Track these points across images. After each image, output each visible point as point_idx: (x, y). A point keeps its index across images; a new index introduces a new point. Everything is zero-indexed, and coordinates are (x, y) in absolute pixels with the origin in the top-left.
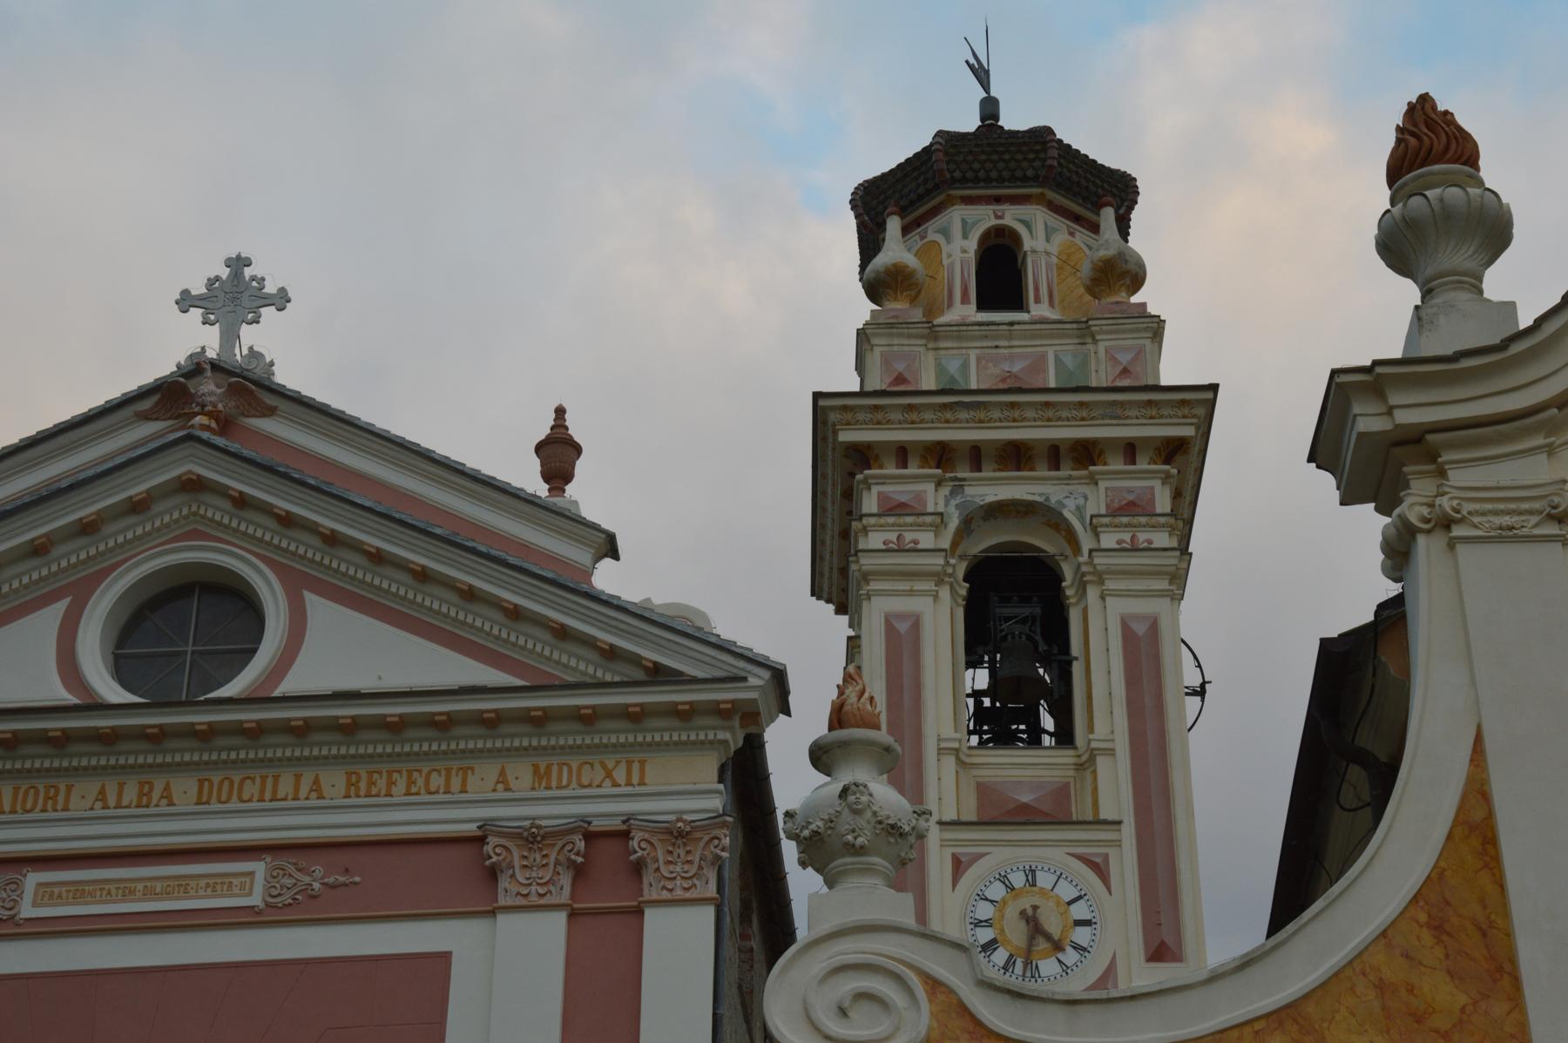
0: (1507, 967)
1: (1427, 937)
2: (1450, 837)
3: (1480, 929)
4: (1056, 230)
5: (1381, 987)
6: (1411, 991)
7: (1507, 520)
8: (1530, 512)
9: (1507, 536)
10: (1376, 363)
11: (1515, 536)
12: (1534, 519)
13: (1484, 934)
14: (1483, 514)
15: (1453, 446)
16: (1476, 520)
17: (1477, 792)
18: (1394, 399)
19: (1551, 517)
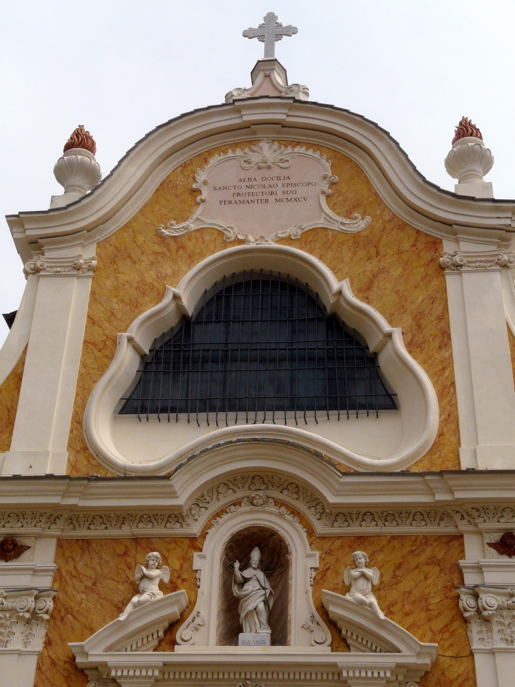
0: (12, 422)
2: (8, 378)
3: (8, 409)
7: (59, 269)
8: (68, 266)
9: (57, 275)
10: (20, 213)
11: (60, 275)
12: (69, 269)
13: (9, 411)
14: (52, 267)
15: (48, 244)
16: (48, 269)
17: (22, 362)
18: (26, 227)
19: (75, 268)
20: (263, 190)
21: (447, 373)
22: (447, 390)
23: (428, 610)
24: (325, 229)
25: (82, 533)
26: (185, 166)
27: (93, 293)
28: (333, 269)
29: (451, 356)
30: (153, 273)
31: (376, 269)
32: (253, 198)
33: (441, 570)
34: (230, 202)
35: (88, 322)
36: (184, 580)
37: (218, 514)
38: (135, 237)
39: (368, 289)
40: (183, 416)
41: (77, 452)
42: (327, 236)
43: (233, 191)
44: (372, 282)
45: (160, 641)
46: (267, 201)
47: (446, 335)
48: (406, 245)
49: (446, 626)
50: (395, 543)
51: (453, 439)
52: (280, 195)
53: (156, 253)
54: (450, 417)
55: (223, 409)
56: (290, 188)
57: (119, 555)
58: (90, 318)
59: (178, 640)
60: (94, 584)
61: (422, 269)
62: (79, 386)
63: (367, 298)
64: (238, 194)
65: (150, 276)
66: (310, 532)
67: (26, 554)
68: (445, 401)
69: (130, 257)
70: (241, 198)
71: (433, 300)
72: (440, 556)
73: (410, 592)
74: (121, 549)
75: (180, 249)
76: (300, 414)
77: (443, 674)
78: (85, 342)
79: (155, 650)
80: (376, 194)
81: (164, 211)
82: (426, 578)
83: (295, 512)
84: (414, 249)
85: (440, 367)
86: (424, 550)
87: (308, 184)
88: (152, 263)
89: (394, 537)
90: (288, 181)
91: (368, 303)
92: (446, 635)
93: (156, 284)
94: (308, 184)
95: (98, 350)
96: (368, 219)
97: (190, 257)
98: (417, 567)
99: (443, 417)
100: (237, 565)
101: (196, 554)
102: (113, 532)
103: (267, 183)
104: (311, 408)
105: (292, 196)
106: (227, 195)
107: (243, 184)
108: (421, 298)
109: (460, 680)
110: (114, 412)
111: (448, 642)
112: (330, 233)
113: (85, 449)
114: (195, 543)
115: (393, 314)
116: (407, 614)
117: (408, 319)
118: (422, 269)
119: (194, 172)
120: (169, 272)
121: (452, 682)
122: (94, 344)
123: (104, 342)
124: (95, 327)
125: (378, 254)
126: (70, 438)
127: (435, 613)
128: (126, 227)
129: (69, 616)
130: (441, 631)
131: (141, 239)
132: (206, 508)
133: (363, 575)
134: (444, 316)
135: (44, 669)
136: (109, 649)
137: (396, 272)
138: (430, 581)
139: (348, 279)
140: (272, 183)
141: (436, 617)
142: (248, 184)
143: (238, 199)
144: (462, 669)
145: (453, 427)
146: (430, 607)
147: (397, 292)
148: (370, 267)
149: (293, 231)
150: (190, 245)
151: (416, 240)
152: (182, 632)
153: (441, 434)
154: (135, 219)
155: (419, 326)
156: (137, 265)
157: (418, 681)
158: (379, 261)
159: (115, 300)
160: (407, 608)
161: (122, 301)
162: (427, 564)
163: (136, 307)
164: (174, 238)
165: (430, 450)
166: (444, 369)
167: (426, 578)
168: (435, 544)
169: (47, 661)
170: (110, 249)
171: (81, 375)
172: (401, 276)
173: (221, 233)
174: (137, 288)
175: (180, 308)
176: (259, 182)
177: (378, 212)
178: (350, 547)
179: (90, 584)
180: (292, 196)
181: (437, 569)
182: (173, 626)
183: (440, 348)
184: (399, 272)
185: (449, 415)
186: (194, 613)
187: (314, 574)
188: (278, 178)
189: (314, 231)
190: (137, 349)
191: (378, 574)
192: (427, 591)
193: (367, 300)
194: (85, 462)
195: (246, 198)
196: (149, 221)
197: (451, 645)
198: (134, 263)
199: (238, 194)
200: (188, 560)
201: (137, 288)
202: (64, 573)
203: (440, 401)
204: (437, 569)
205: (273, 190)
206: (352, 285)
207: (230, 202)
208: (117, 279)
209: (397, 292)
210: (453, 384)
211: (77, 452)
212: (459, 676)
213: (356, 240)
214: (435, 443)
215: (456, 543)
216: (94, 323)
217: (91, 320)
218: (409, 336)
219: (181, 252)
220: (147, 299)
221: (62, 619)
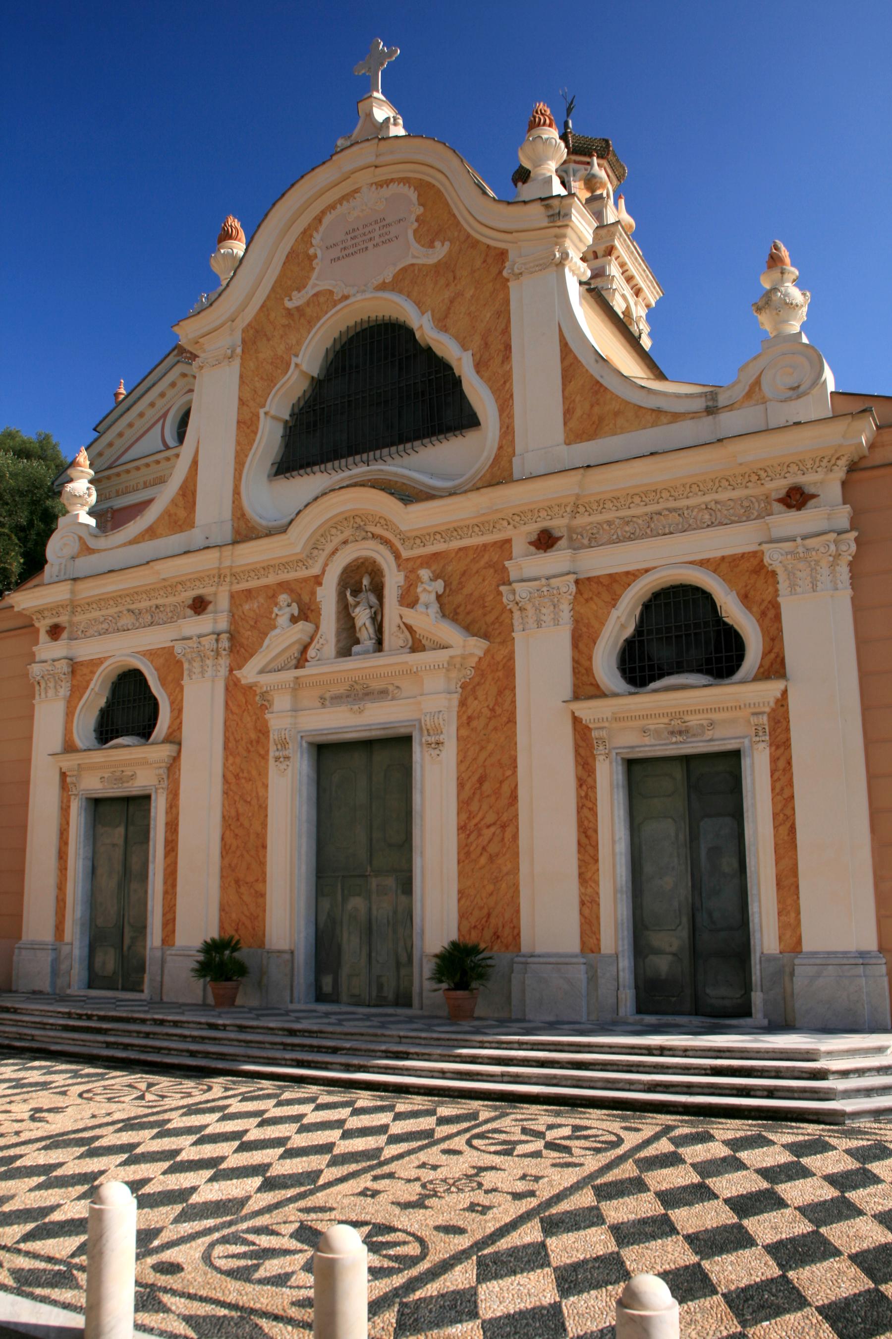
1: (181, 499)
4: (578, 171)
5: (170, 515)
6: (176, 514)
20: (365, 238)
21: (508, 384)
22: (505, 404)
23: (484, 607)
24: (413, 265)
25: (244, 586)
26: (304, 232)
27: (241, 377)
28: (418, 304)
29: (511, 368)
30: (282, 347)
31: (453, 295)
32: (356, 249)
33: (496, 571)
34: (339, 258)
35: (239, 404)
36: (312, 611)
37: (334, 553)
38: (268, 315)
39: (446, 317)
40: (316, 468)
41: (239, 519)
42: (414, 271)
43: (342, 246)
44: (449, 308)
45: (299, 661)
46: (367, 248)
47: (508, 347)
48: (478, 263)
49: (497, 618)
50: (461, 554)
51: (510, 450)
52: (377, 240)
53: (283, 326)
54: (507, 430)
55: (350, 454)
56: (385, 230)
57: (270, 598)
58: (240, 399)
59: (309, 659)
60: (256, 623)
61: (491, 284)
62: (236, 463)
63: (445, 326)
64: (345, 248)
65: (281, 349)
66: (397, 556)
67: (210, 608)
68: (505, 414)
69: (266, 335)
70: (347, 252)
71: (498, 314)
72: (495, 560)
73: (471, 594)
74: (270, 593)
75: (302, 318)
76: (409, 445)
77: (493, 658)
78: (239, 422)
79: (296, 668)
80: (454, 215)
81: (289, 283)
82: (484, 580)
83: (386, 542)
84: (485, 265)
85: (502, 382)
86: (483, 556)
87: (400, 221)
88: (282, 337)
89: (460, 549)
90: (384, 223)
91: (446, 331)
92: (497, 625)
93: (285, 356)
94: (400, 221)
95: (247, 426)
96: (447, 244)
97: (309, 322)
98: (477, 572)
99: (503, 430)
100: (348, 594)
101: (318, 589)
102: (264, 581)
103: (367, 230)
104: (417, 438)
105: (387, 237)
106: (335, 252)
107: (349, 237)
108: (488, 315)
109: (505, 661)
110: (269, 476)
111: (498, 632)
112: (417, 268)
113: (243, 515)
114: (317, 580)
115: (465, 338)
116: (468, 613)
117: (477, 340)
118: (491, 284)
119: (311, 236)
120: (294, 342)
121: (498, 663)
122: (244, 423)
123: (251, 419)
124: (245, 408)
125: (454, 278)
126: (233, 508)
127: (488, 609)
128: (263, 306)
129: (242, 649)
130: (493, 623)
131: (273, 315)
132: (323, 550)
133: (425, 590)
134: (506, 331)
135: (230, 689)
136: (261, 672)
137: (469, 294)
138: (486, 582)
139: (429, 313)
140: (370, 228)
141: (490, 612)
142: (352, 235)
143: (347, 252)
144: (507, 651)
145: (510, 438)
146: (486, 604)
147: (469, 314)
148: (447, 294)
149: (388, 275)
150: (308, 311)
151: (487, 255)
152: (311, 653)
153: (500, 447)
154: (268, 297)
155: (486, 344)
156: (271, 342)
157: (474, 665)
158: (456, 285)
159: (256, 379)
160: (469, 607)
161: (262, 378)
162: (485, 568)
163: (271, 381)
164: (298, 308)
165: (492, 463)
166: (505, 383)
167: (484, 580)
168: (491, 549)
169: (231, 683)
170: (251, 332)
171: (237, 452)
172: (472, 296)
173: (331, 292)
174: (272, 363)
175: (304, 373)
176: (361, 231)
177: (456, 234)
178: (427, 563)
179: (252, 623)
180: (387, 237)
181: (492, 571)
182: (305, 648)
183: (503, 362)
184: (471, 293)
185: (508, 428)
186: (318, 636)
187: (400, 592)
188: (376, 222)
189: (404, 270)
190: (275, 418)
191: (443, 584)
192: (484, 591)
193: (444, 329)
194: (244, 526)
195: (352, 250)
196: (278, 296)
197: (500, 633)
198: (268, 340)
199: (345, 248)
200: (313, 593)
201: (272, 363)
202: (236, 617)
203: (500, 415)
204: (492, 571)
205: (372, 235)
206: (433, 316)
207: (339, 258)
208: (257, 358)
209: (469, 314)
210: (512, 396)
211: (239, 519)
212: (504, 657)
213: (439, 269)
214: (496, 456)
215: (507, 546)
216: (243, 404)
217: (242, 402)
218: (478, 356)
219: (302, 320)
220: (279, 371)
221: (238, 651)
